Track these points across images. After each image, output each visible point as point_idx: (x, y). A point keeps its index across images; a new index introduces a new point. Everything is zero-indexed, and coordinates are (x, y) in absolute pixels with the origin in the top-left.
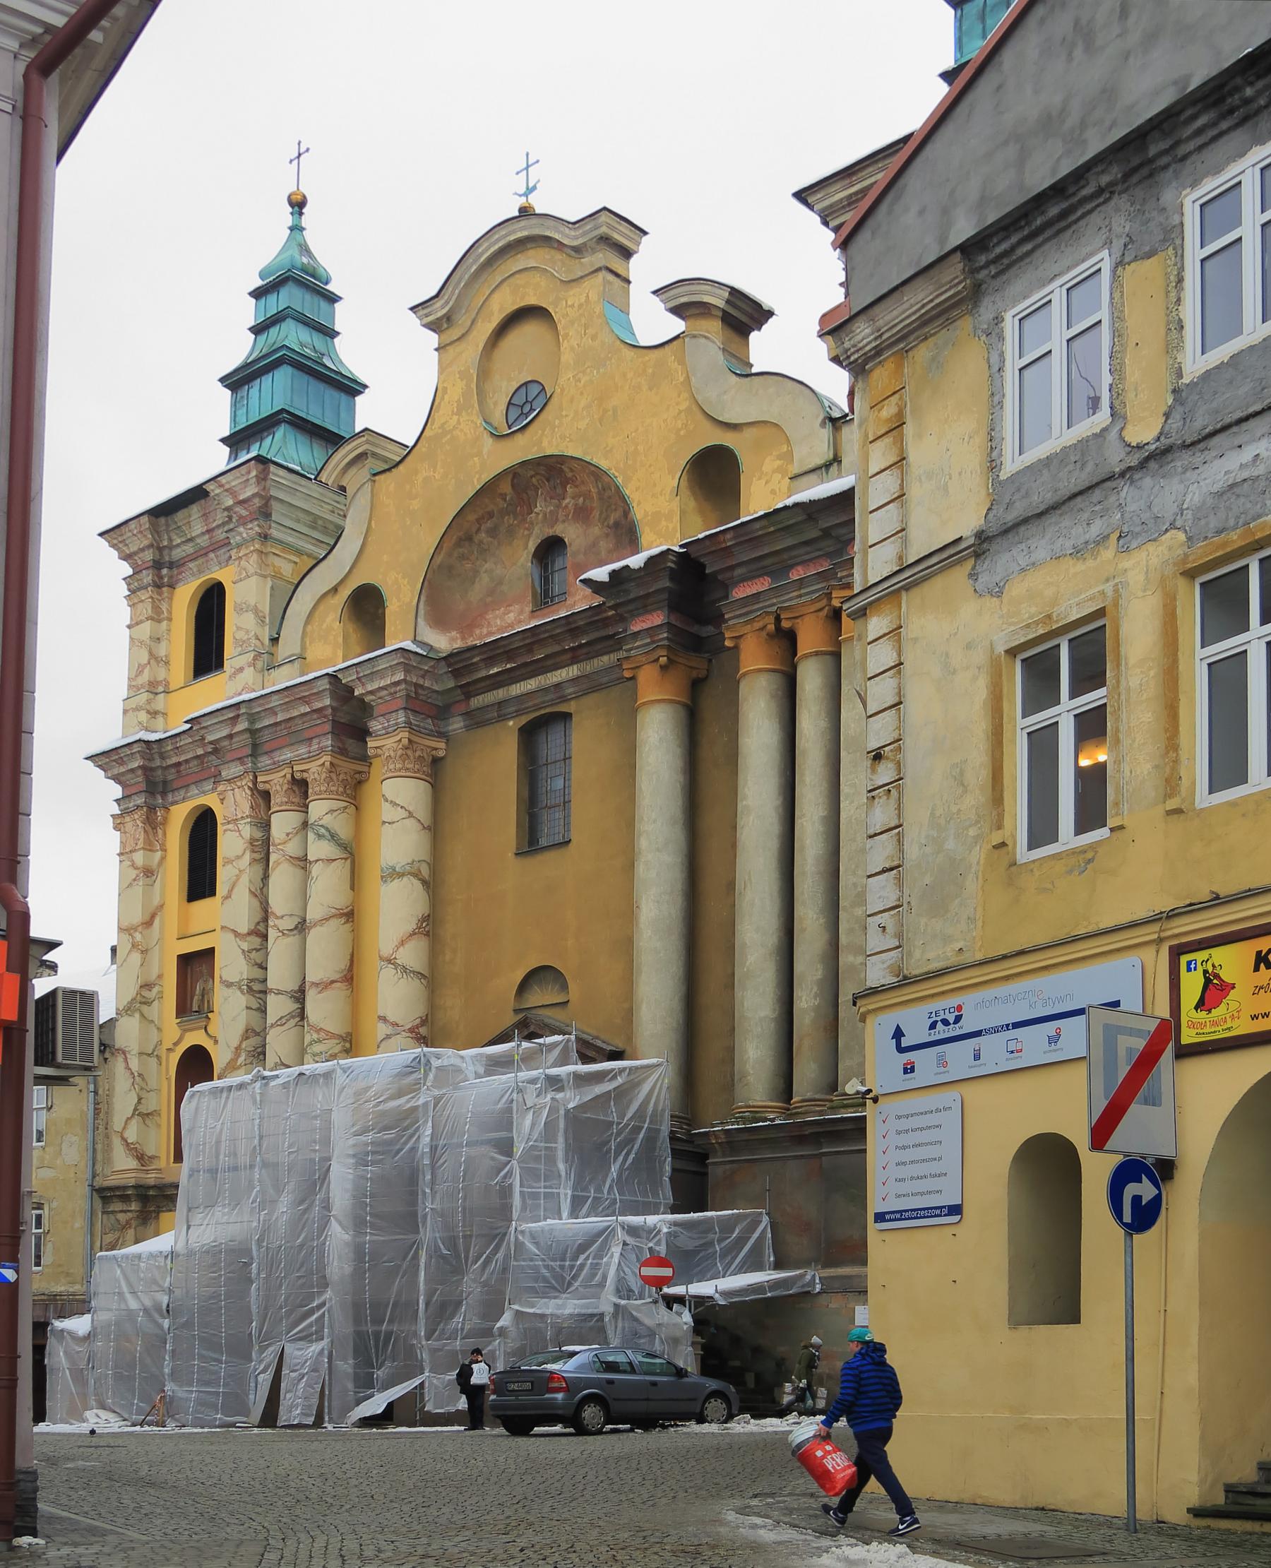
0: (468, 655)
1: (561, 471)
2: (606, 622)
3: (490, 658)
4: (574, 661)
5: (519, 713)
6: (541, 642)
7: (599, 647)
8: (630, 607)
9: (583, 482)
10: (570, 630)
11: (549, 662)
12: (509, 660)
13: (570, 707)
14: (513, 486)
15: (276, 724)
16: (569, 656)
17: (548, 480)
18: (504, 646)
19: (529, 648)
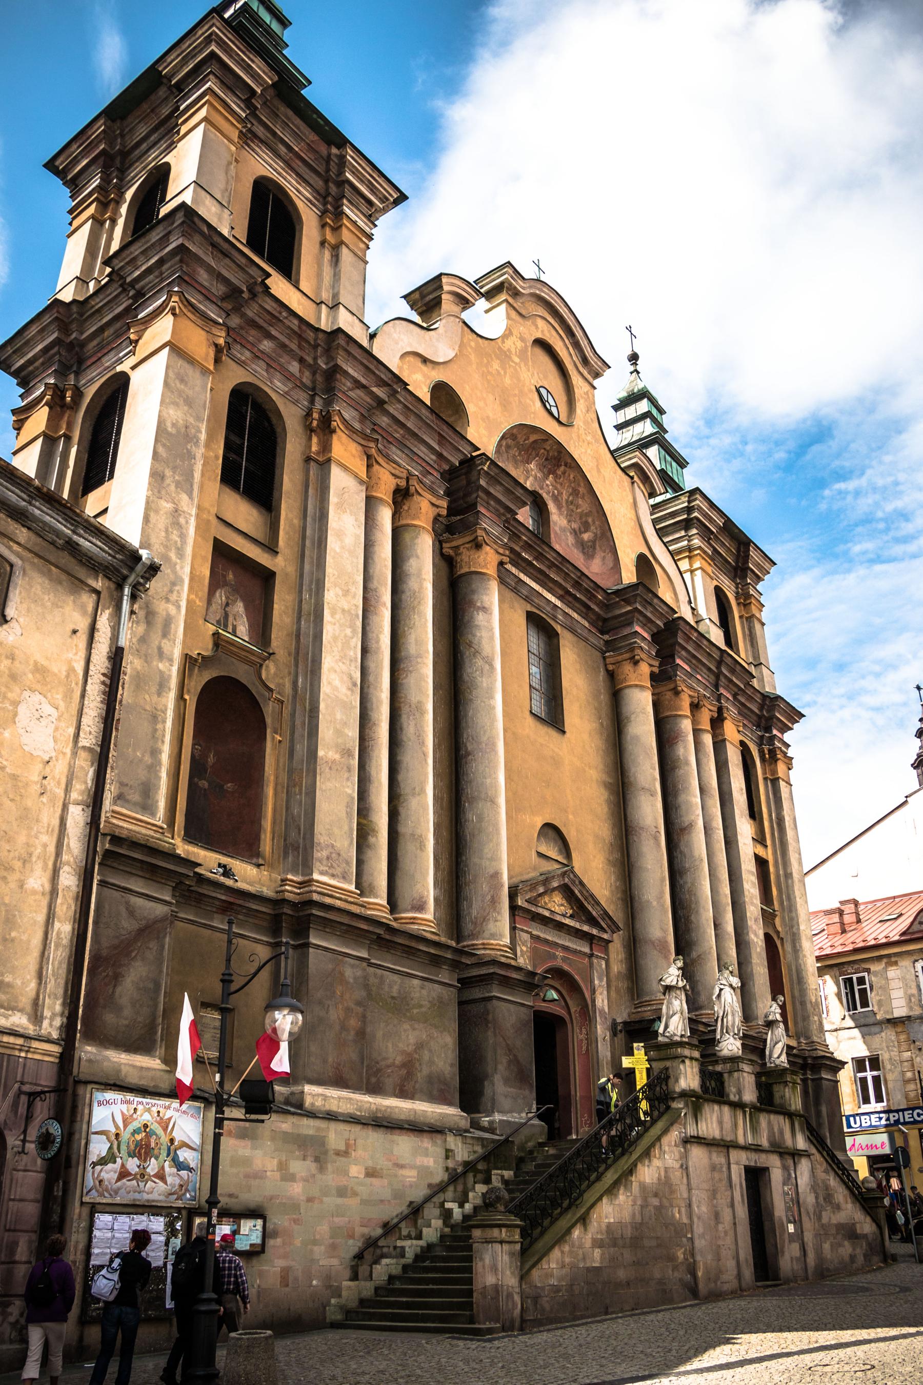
0: (522, 530)
1: (559, 466)
2: (592, 597)
3: (530, 546)
4: (560, 598)
5: (527, 599)
6: (559, 570)
7: (577, 605)
8: (641, 618)
9: (561, 484)
10: (577, 582)
11: (551, 585)
12: (536, 558)
13: (558, 629)
14: (535, 442)
15: (402, 425)
16: (561, 592)
17: (546, 459)
18: (543, 550)
19: (552, 565)
